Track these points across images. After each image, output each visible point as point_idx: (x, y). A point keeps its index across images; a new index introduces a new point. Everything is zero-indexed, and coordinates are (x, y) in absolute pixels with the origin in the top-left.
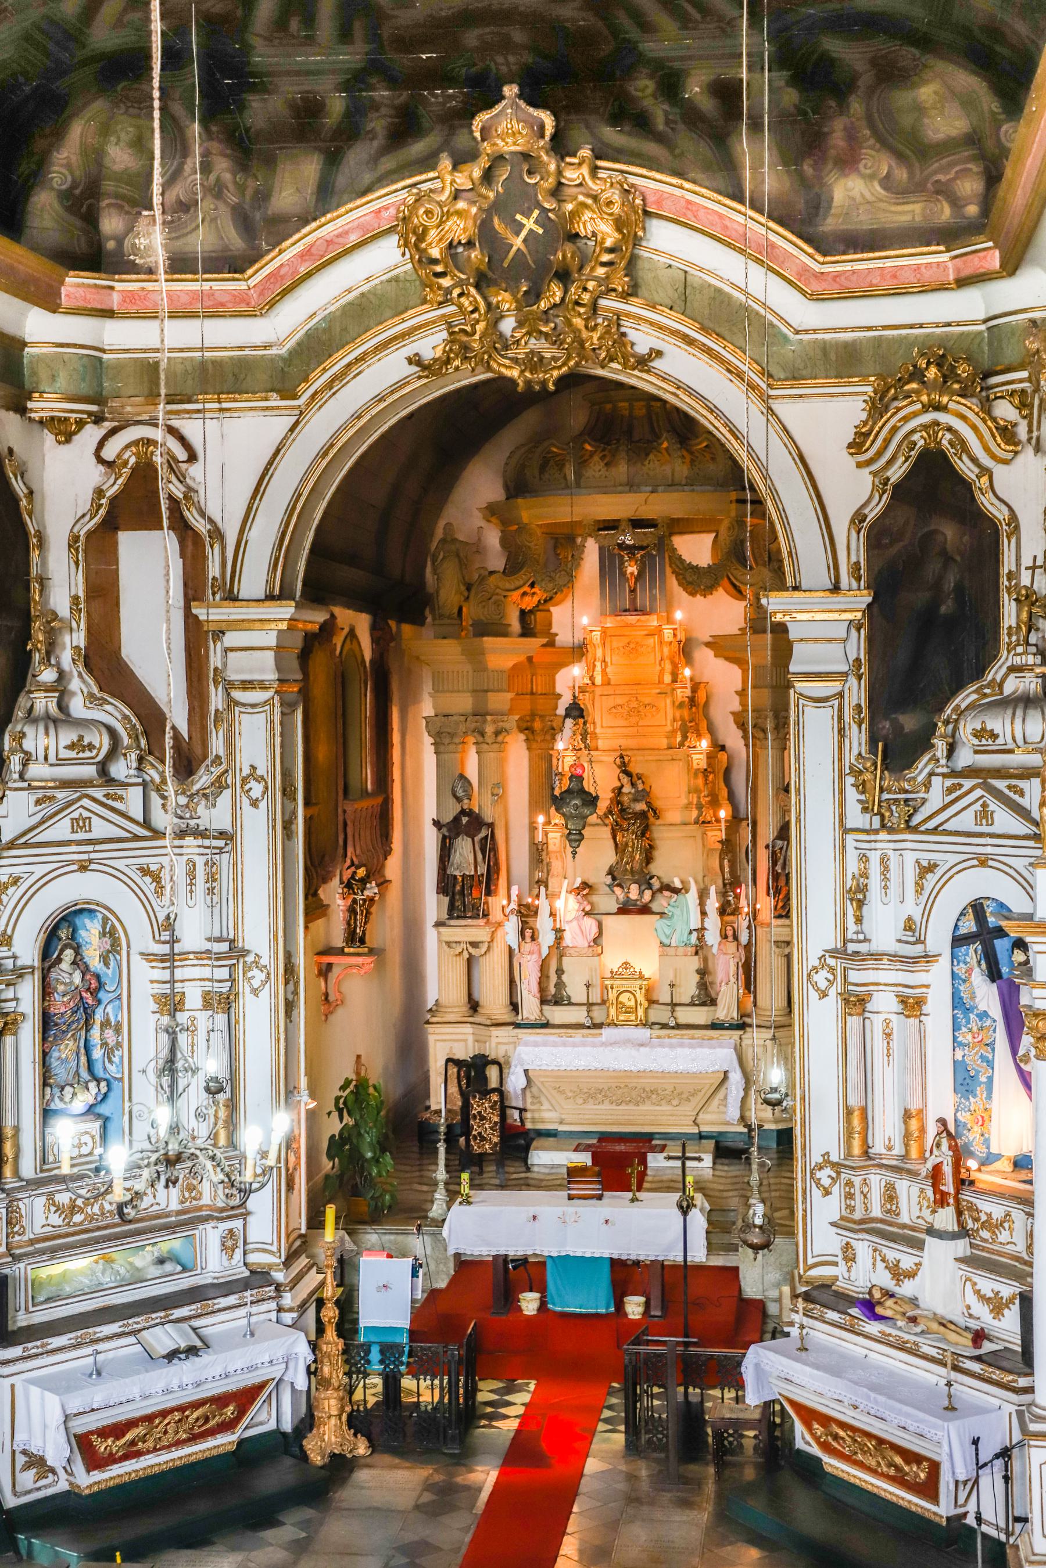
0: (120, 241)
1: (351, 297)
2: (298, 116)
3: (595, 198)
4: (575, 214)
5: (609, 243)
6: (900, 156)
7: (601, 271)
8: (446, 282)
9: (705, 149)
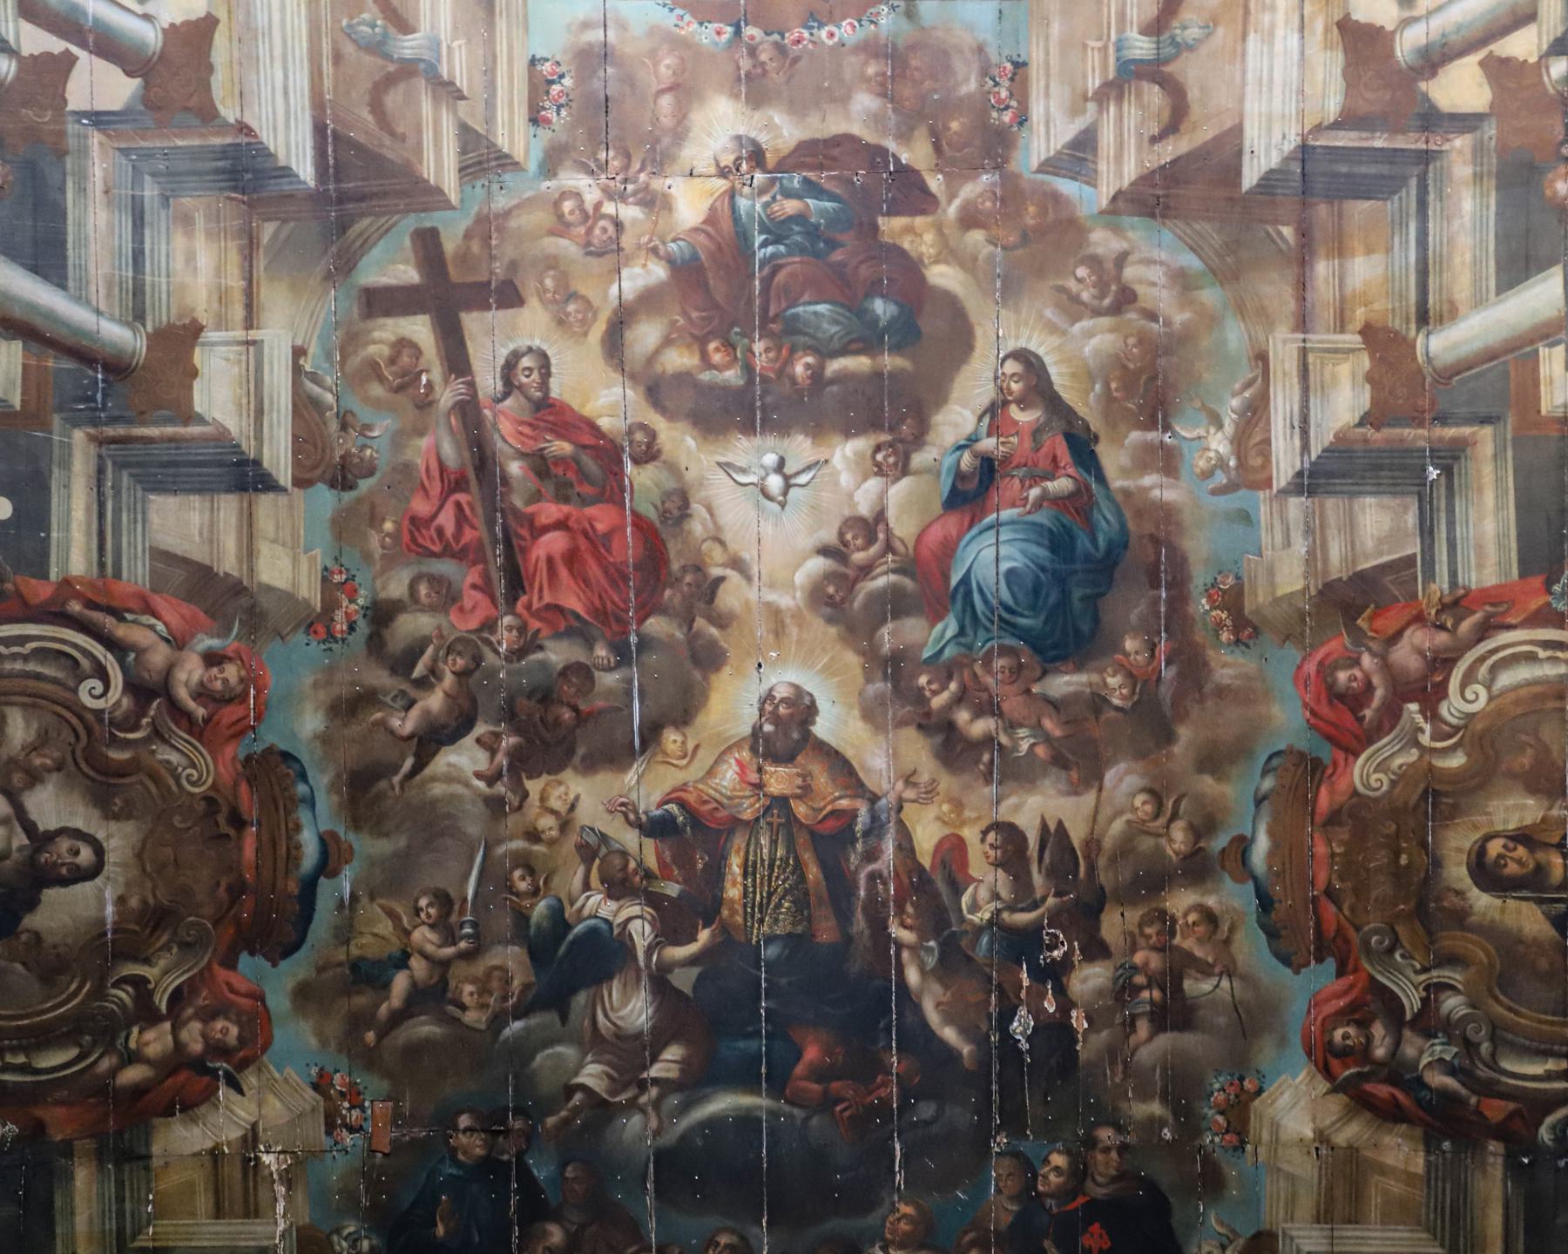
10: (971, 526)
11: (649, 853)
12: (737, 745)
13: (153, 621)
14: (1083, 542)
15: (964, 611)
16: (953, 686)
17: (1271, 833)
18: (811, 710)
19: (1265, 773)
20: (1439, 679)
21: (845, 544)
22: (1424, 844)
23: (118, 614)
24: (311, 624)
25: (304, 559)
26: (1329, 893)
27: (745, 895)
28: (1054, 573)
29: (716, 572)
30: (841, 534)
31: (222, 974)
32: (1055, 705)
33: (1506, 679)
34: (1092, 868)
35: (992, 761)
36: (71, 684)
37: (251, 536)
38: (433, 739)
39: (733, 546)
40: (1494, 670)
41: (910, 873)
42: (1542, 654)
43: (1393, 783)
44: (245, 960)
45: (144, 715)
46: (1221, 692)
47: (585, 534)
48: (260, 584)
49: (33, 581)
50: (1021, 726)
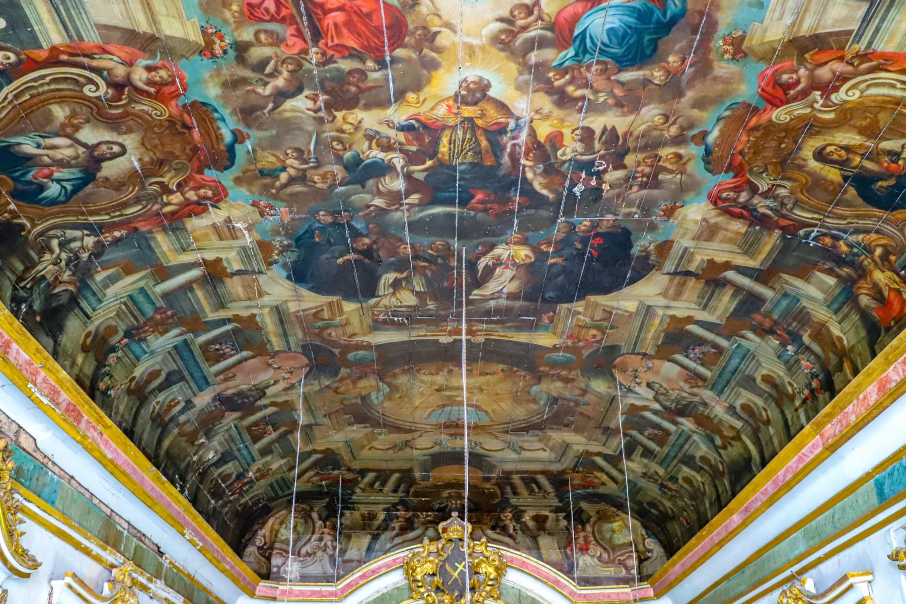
0: (279, 567)
1: (378, 595)
2: (364, 520)
3: (487, 558)
4: (479, 564)
5: (492, 577)
6: (605, 549)
7: (488, 588)
8: (422, 590)
9: (528, 541)
10: (591, 8)
11: (402, 137)
12: (448, 99)
13: (111, 56)
14: (658, 14)
15: (580, 46)
16: (567, 77)
17: (721, 131)
18: (488, 86)
19: (726, 110)
20: (837, 84)
21: (514, 16)
22: (796, 142)
23: (90, 56)
24: (201, 52)
25: (188, 24)
26: (741, 153)
27: (450, 150)
28: (636, 29)
29: (435, 29)
30: (511, 12)
31: (198, 177)
32: (622, 84)
33: (873, 91)
34: (625, 141)
35: (583, 106)
36: (78, 89)
37: (152, 14)
38: (281, 96)
39: (445, 17)
40: (869, 86)
41: (533, 143)
42: (899, 85)
43: (792, 119)
44: (206, 171)
45: (123, 94)
46: (715, 79)
47: (355, 12)
48: (166, 36)
49: (35, 51)
50: (601, 92)
